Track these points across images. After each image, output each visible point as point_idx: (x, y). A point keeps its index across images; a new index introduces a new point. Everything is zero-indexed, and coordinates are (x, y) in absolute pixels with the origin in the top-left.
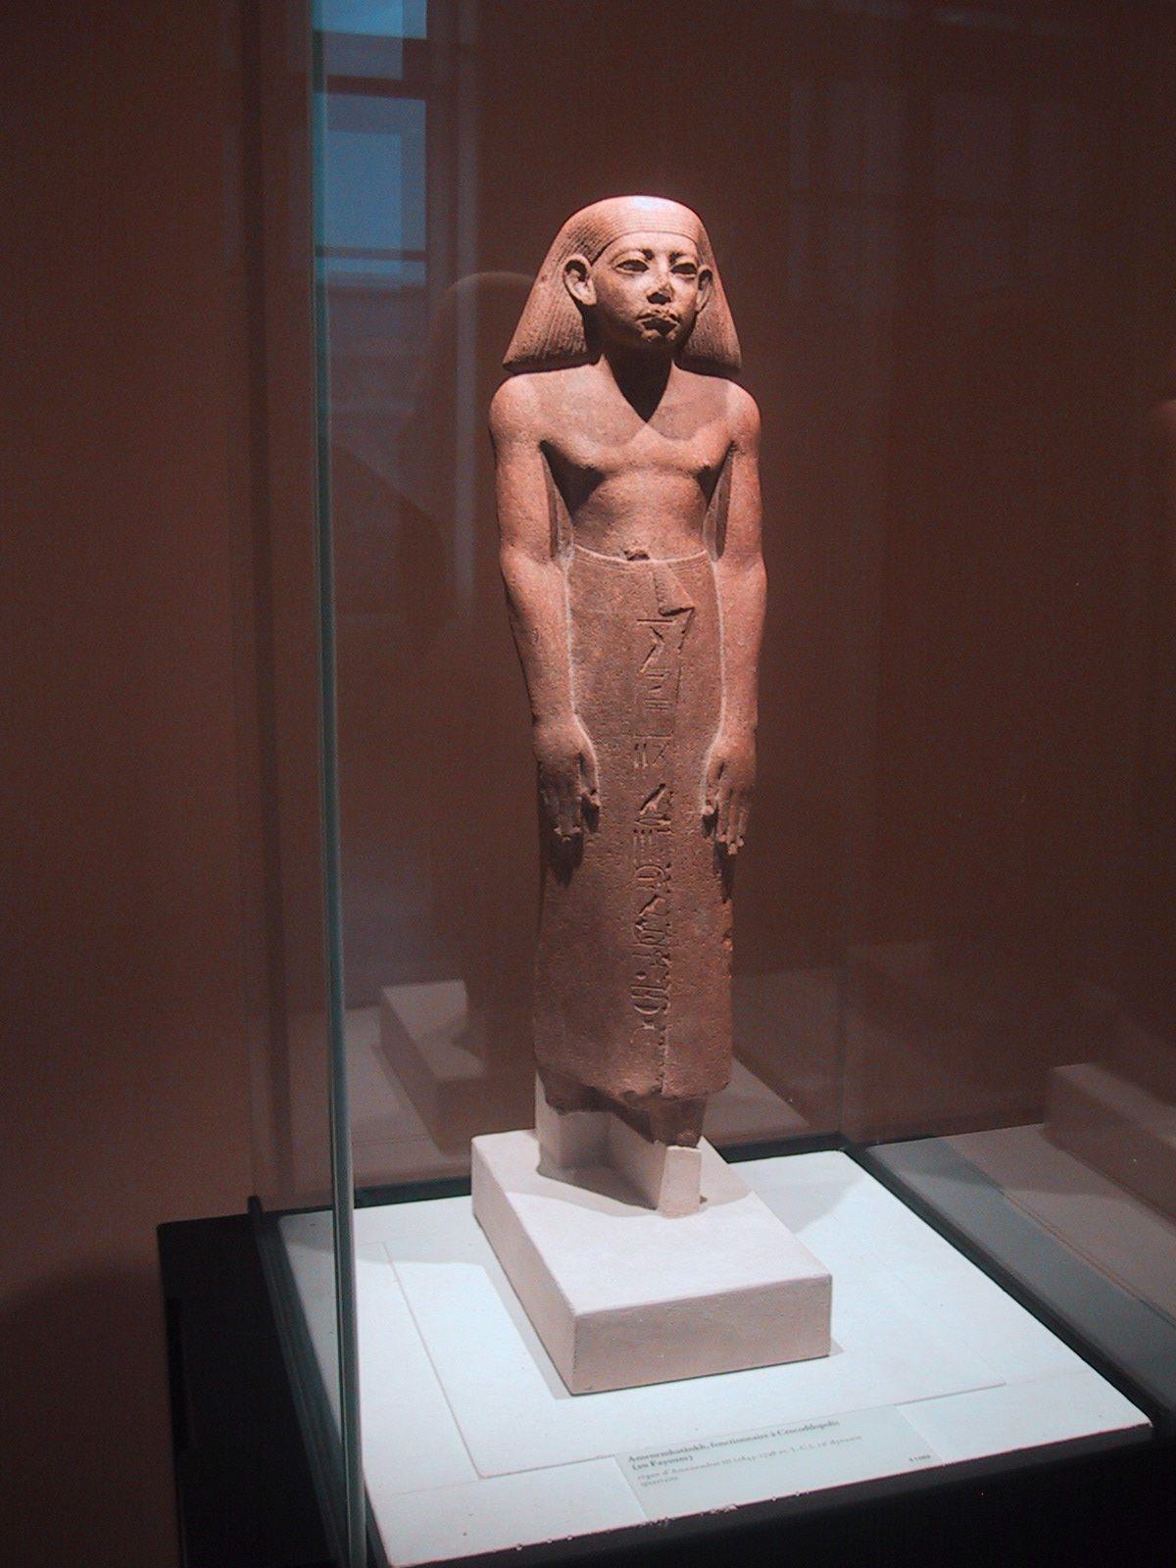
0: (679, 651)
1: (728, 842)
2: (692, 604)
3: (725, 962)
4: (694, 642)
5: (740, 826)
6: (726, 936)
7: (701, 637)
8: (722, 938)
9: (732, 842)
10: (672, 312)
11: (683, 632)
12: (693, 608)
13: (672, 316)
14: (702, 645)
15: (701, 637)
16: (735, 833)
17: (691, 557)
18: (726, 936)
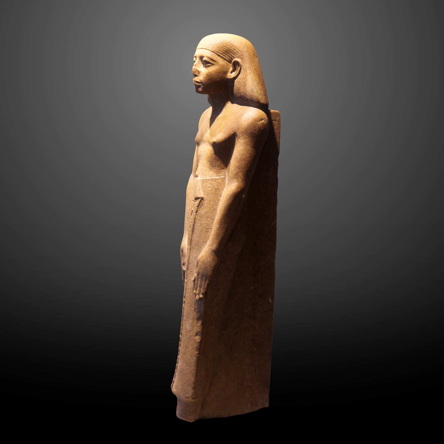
0: (195, 214)
1: (197, 294)
2: (202, 196)
3: (195, 345)
4: (202, 211)
5: (202, 289)
6: (197, 334)
7: (205, 210)
8: (195, 334)
9: (198, 294)
10: (197, 80)
11: (198, 207)
12: (202, 199)
13: (197, 82)
14: (204, 213)
15: (205, 210)
16: (200, 291)
17: (209, 178)
18: (197, 334)
